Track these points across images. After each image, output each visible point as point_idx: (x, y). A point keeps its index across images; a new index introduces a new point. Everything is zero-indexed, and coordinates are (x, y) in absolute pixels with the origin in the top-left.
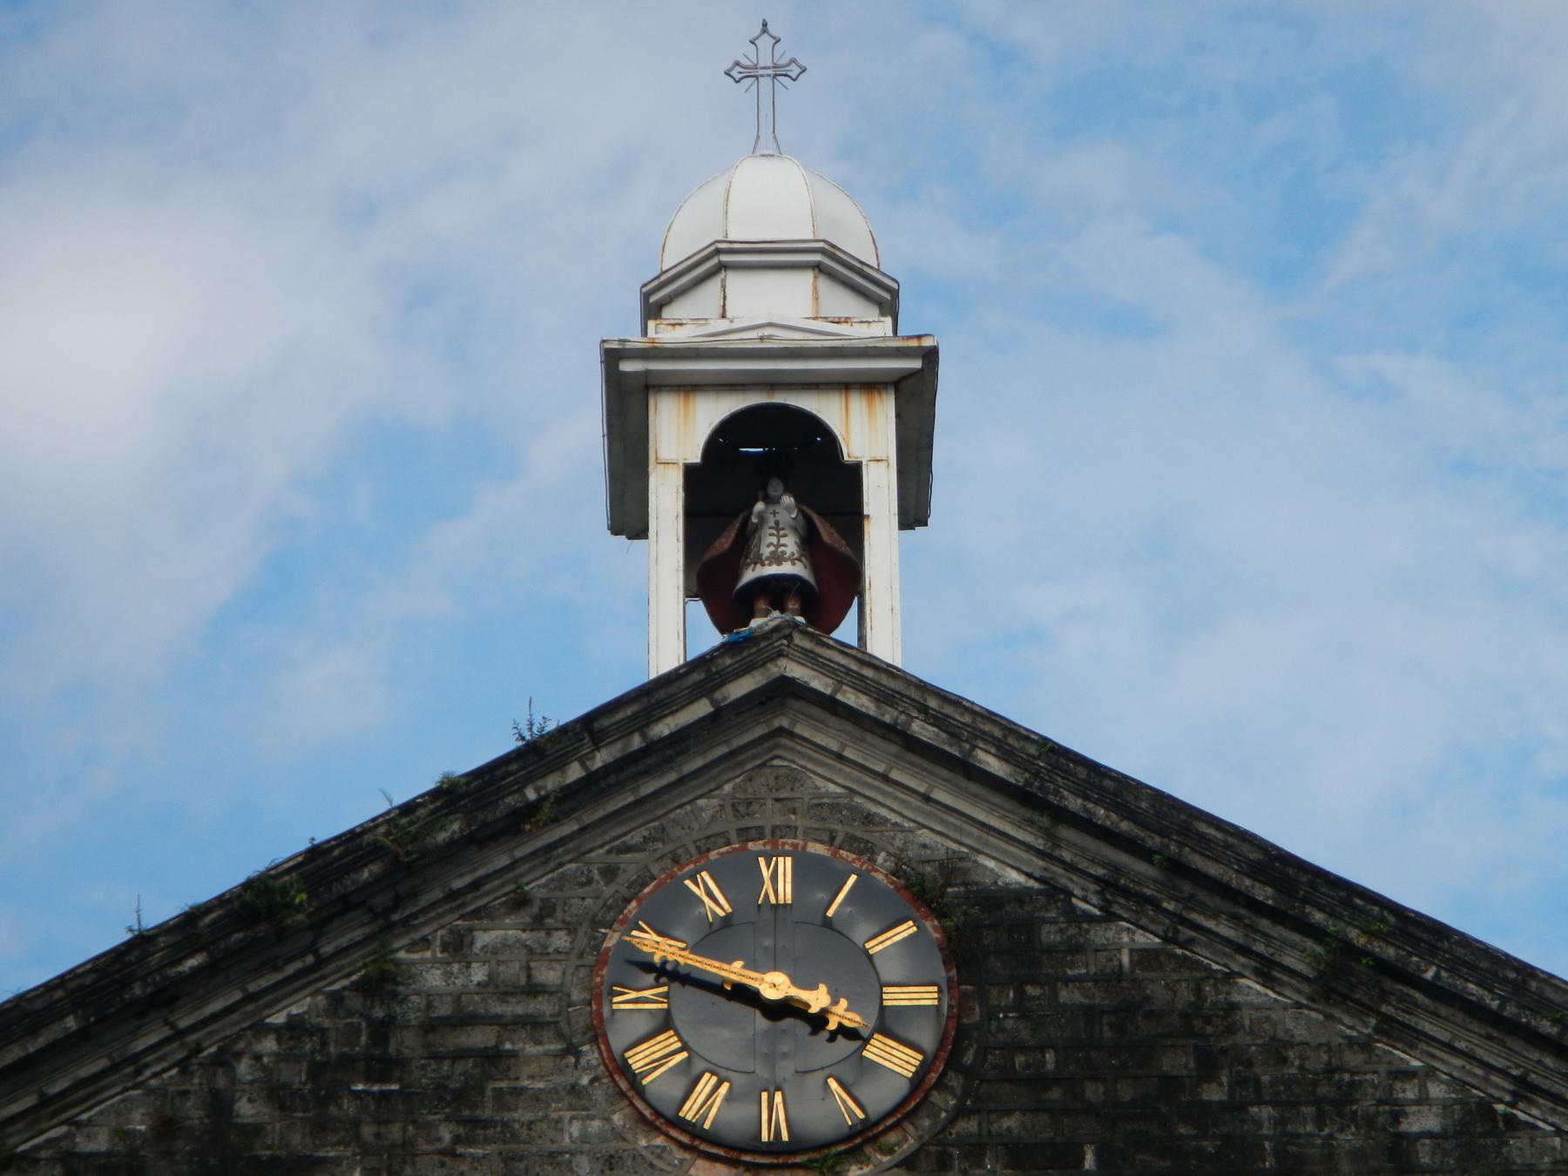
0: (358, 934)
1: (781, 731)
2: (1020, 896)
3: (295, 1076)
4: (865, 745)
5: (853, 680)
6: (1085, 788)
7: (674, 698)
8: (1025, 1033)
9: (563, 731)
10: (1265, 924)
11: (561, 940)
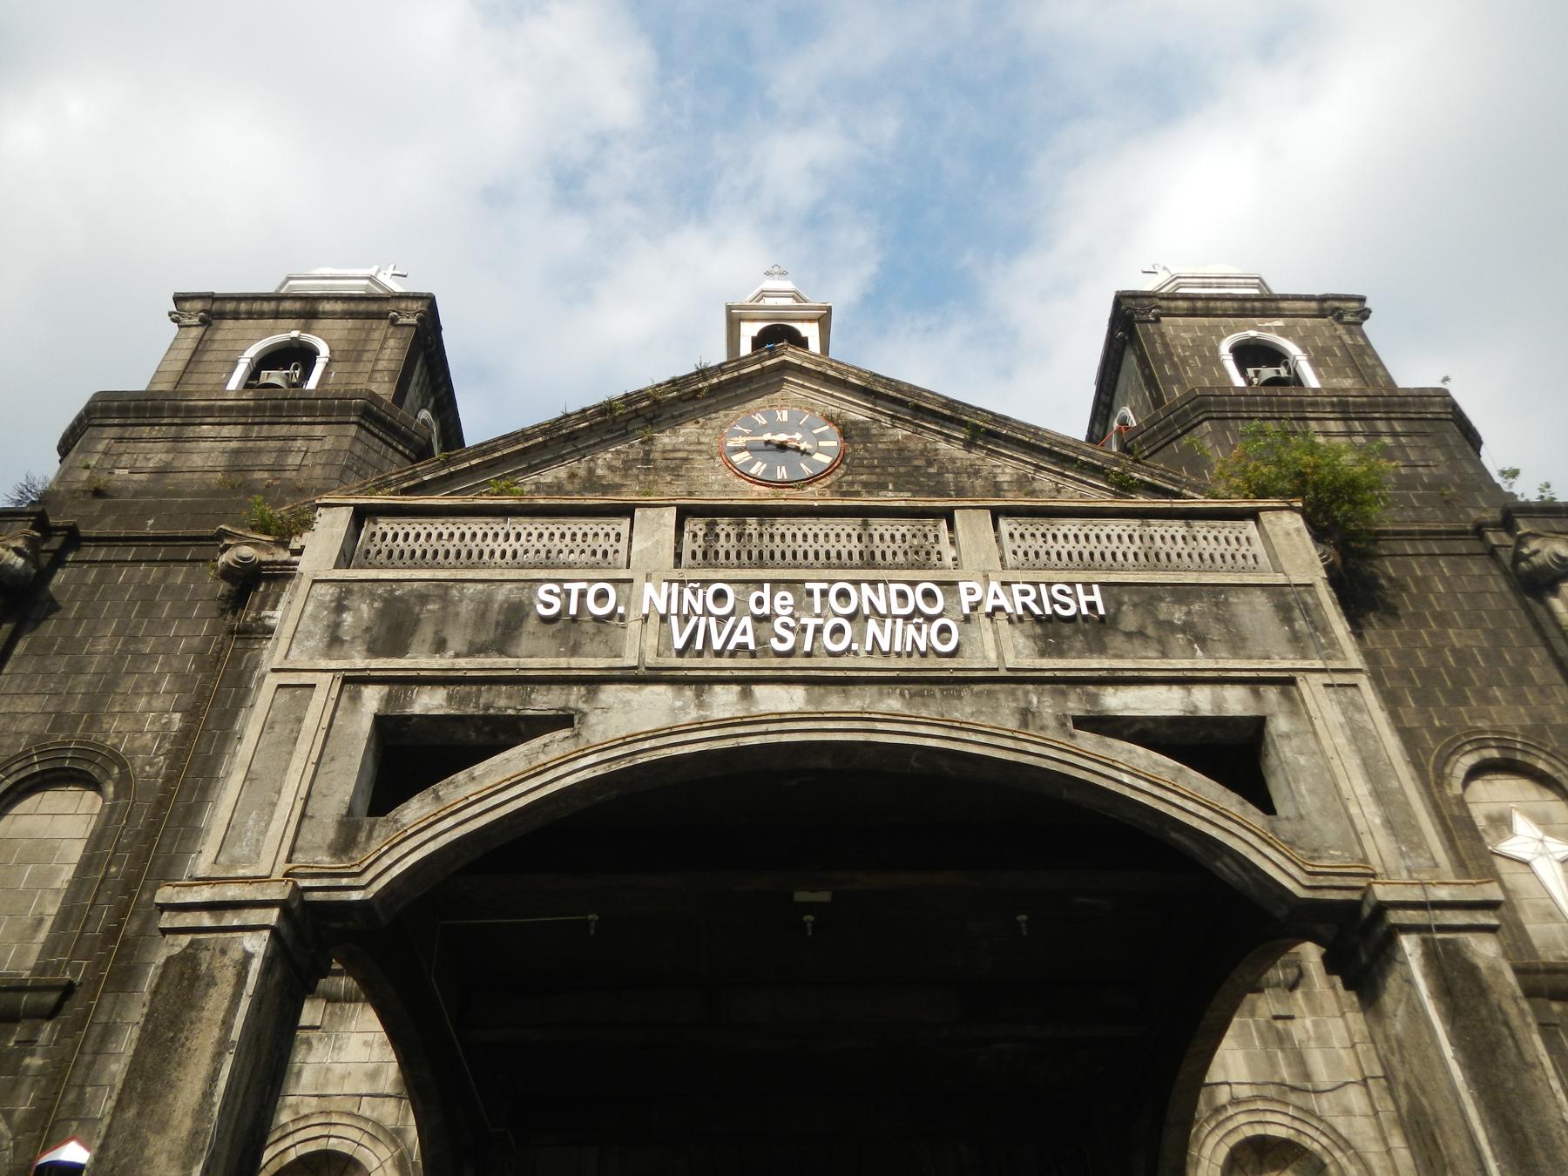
0: (641, 425)
1: (785, 367)
2: (864, 422)
3: (618, 463)
8: (867, 455)
9: (711, 368)
10: (947, 424)
11: (709, 431)
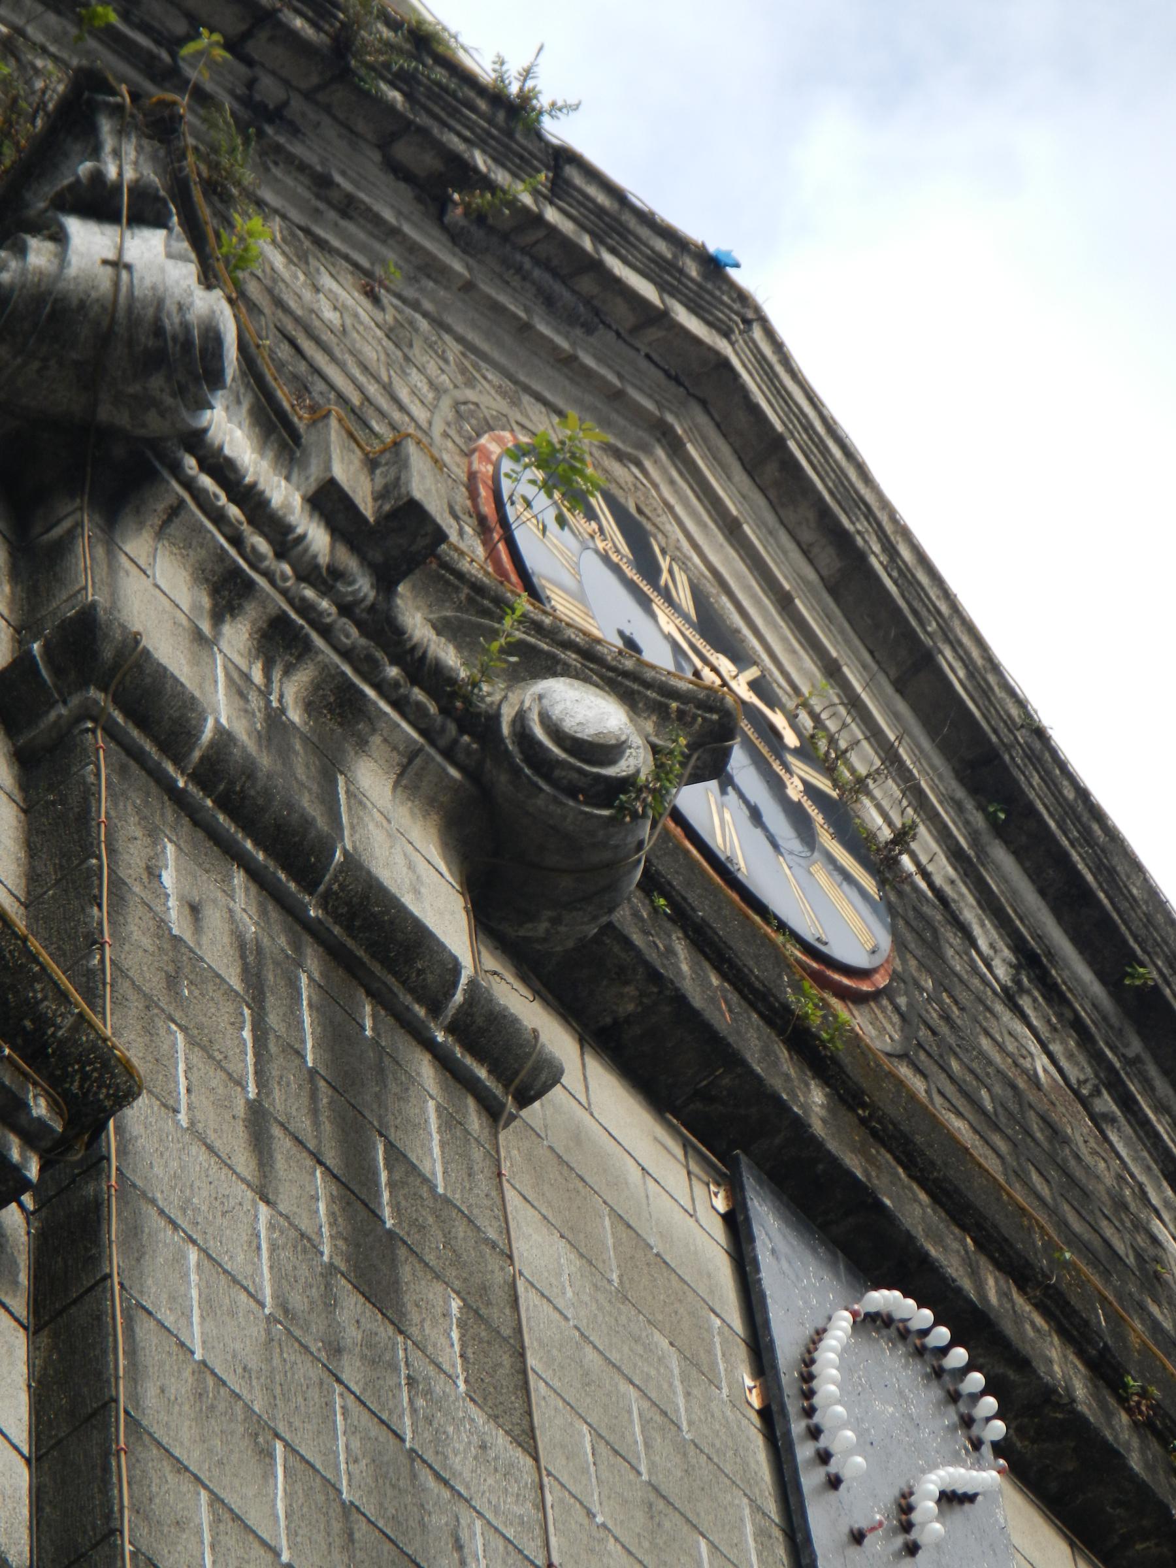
4: (771, 540)
5: (810, 443)
6: (1066, 813)
7: (638, 243)
